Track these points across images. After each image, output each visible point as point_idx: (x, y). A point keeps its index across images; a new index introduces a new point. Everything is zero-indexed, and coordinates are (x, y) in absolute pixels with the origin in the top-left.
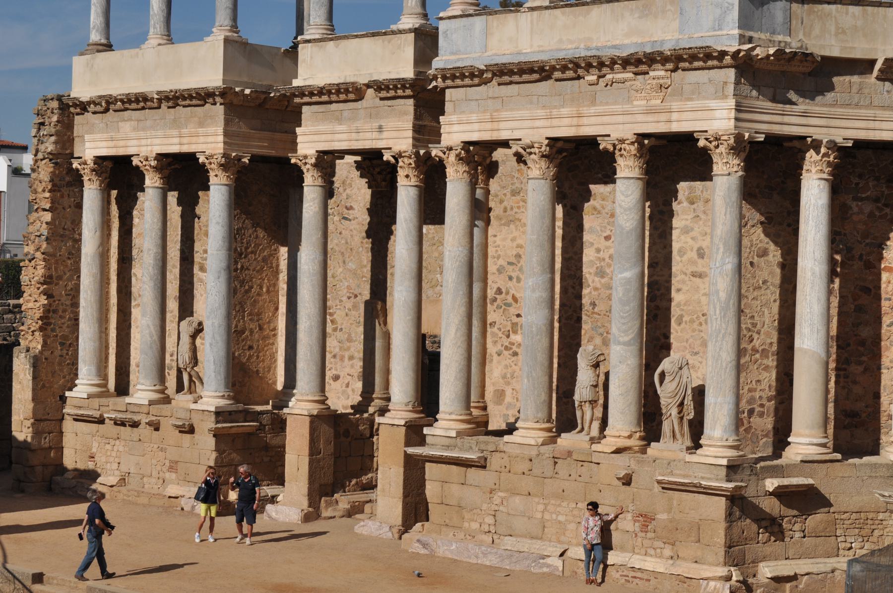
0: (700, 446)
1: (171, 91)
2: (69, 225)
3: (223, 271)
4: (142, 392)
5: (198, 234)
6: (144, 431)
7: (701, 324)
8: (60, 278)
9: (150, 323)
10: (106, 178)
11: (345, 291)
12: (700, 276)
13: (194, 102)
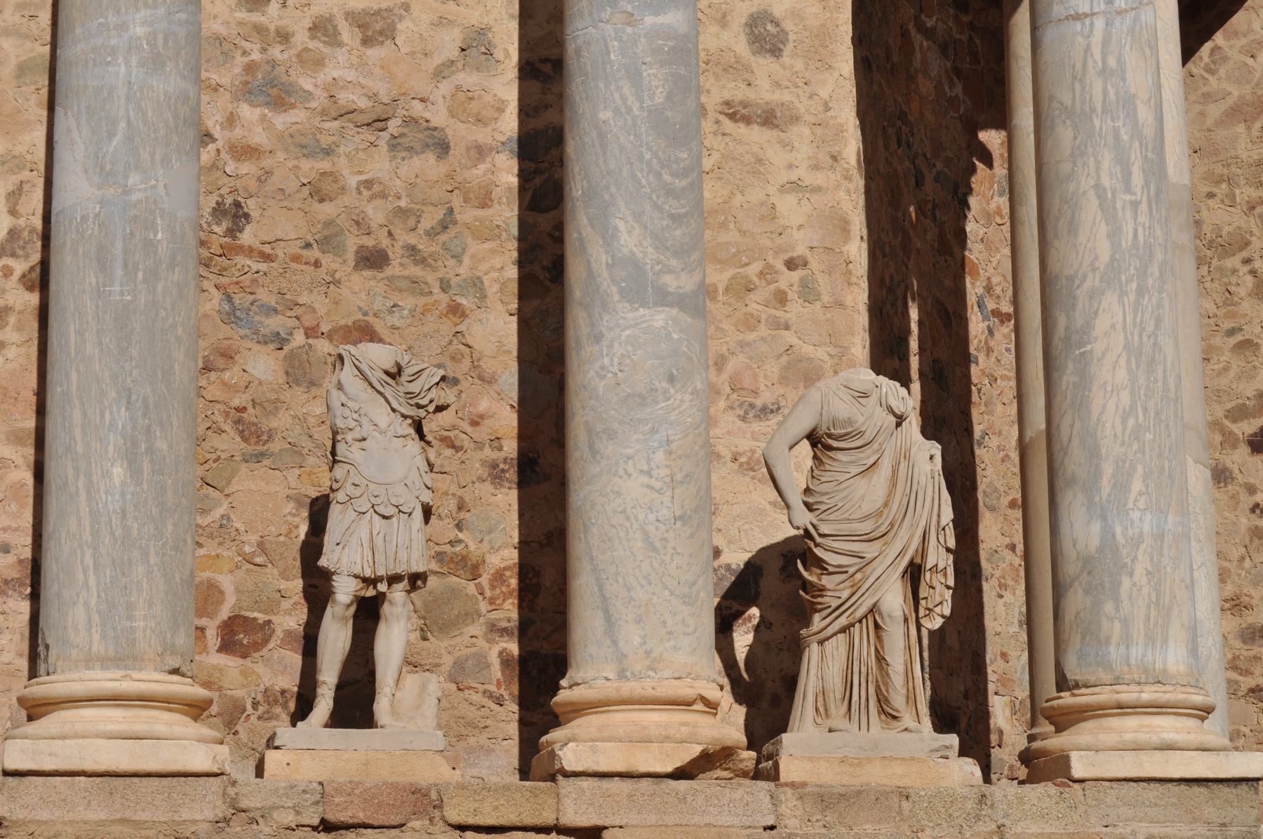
7: (781, 298)
12: (769, 119)
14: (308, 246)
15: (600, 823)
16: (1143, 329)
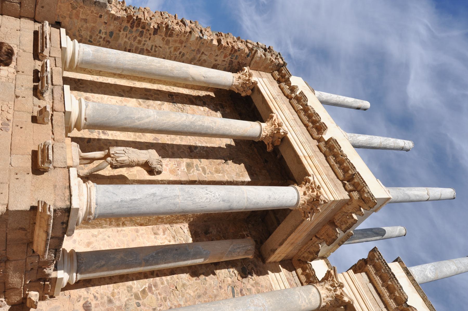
1: (341, 151)
2: (204, 57)
3: (229, 204)
4: (75, 103)
5: (214, 162)
6: (32, 105)
8: (168, 42)
9: (151, 119)
10: (238, 90)
11: (176, 303)
13: (340, 172)
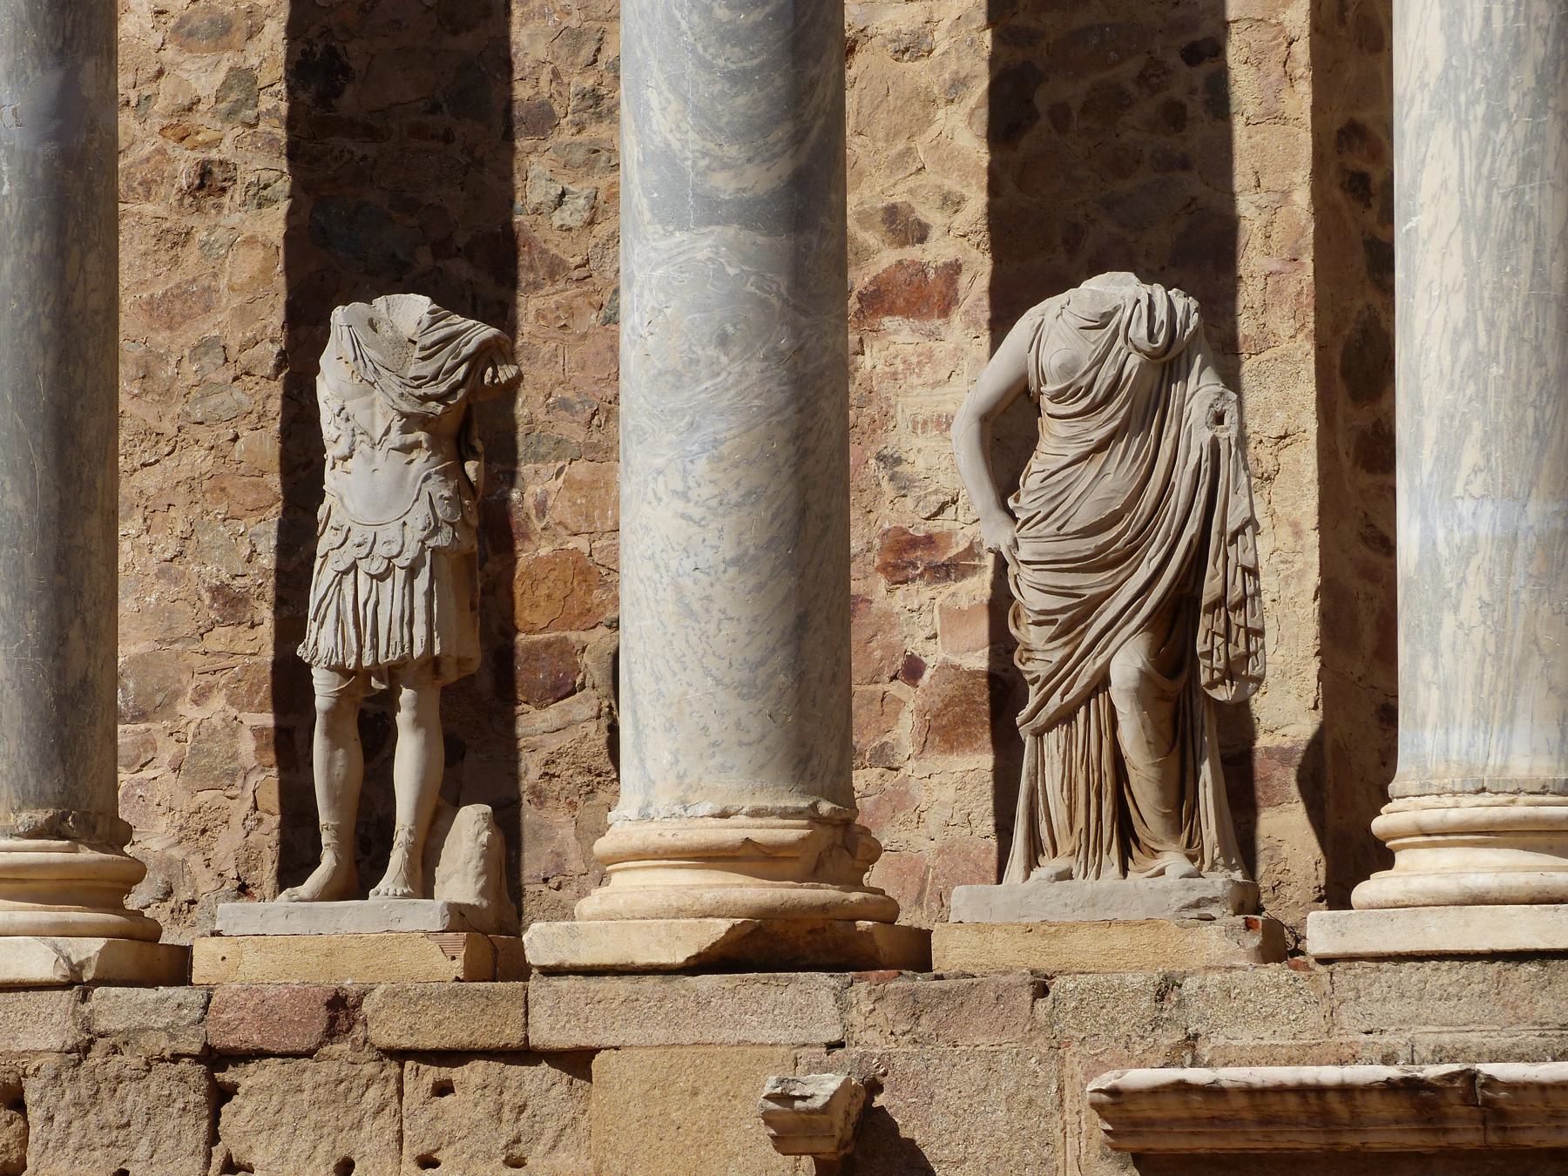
0: (1382, 857)
14: (435, 108)
15: (584, 1042)
16: (1492, 185)
